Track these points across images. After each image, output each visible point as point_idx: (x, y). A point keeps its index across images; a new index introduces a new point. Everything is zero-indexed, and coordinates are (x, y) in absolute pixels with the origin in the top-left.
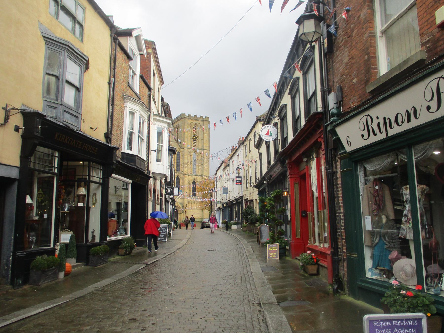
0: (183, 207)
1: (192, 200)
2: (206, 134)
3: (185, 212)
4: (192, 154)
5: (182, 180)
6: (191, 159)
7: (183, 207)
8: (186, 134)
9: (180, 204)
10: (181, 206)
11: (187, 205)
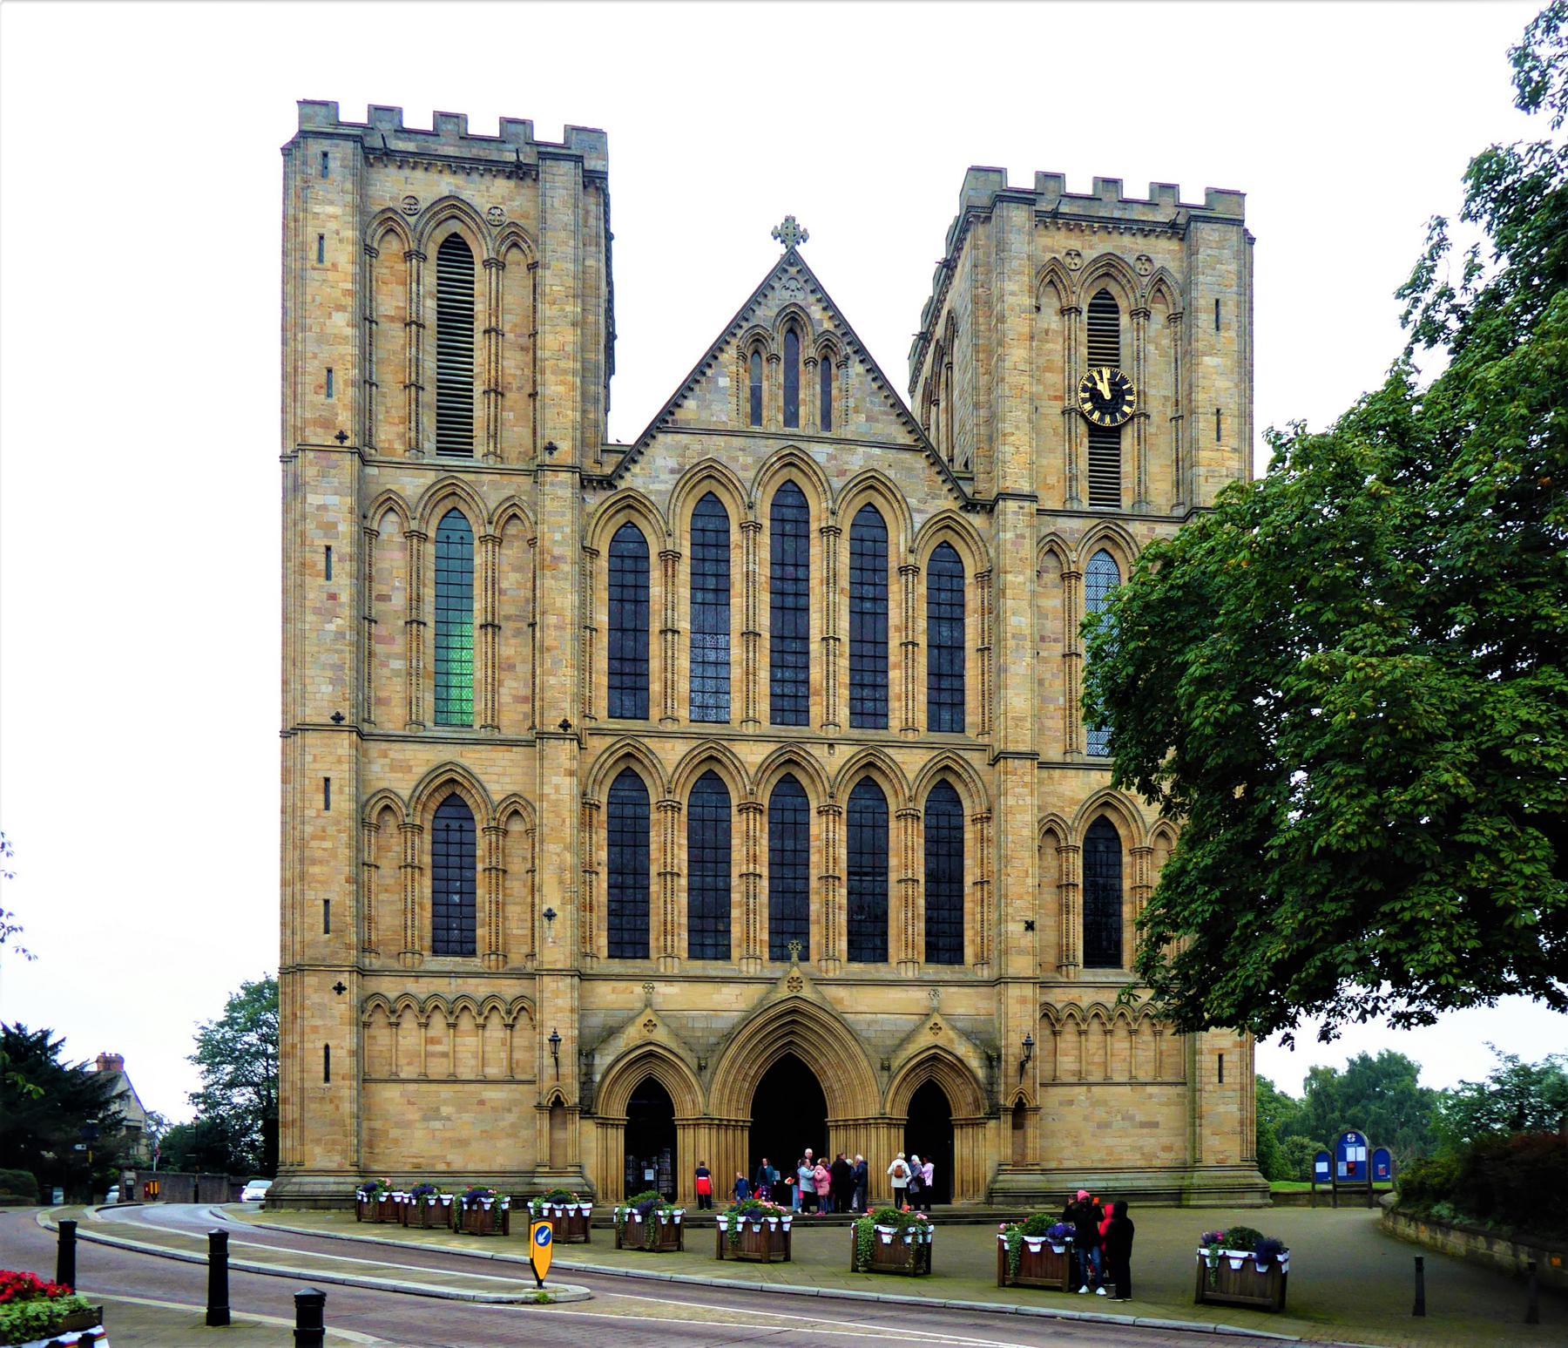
0: (992, 1060)
1: (1086, 998)
4: (1079, 558)
5: (980, 810)
6: (1069, 608)
7: (992, 1060)
9: (967, 1035)
10: (975, 1063)
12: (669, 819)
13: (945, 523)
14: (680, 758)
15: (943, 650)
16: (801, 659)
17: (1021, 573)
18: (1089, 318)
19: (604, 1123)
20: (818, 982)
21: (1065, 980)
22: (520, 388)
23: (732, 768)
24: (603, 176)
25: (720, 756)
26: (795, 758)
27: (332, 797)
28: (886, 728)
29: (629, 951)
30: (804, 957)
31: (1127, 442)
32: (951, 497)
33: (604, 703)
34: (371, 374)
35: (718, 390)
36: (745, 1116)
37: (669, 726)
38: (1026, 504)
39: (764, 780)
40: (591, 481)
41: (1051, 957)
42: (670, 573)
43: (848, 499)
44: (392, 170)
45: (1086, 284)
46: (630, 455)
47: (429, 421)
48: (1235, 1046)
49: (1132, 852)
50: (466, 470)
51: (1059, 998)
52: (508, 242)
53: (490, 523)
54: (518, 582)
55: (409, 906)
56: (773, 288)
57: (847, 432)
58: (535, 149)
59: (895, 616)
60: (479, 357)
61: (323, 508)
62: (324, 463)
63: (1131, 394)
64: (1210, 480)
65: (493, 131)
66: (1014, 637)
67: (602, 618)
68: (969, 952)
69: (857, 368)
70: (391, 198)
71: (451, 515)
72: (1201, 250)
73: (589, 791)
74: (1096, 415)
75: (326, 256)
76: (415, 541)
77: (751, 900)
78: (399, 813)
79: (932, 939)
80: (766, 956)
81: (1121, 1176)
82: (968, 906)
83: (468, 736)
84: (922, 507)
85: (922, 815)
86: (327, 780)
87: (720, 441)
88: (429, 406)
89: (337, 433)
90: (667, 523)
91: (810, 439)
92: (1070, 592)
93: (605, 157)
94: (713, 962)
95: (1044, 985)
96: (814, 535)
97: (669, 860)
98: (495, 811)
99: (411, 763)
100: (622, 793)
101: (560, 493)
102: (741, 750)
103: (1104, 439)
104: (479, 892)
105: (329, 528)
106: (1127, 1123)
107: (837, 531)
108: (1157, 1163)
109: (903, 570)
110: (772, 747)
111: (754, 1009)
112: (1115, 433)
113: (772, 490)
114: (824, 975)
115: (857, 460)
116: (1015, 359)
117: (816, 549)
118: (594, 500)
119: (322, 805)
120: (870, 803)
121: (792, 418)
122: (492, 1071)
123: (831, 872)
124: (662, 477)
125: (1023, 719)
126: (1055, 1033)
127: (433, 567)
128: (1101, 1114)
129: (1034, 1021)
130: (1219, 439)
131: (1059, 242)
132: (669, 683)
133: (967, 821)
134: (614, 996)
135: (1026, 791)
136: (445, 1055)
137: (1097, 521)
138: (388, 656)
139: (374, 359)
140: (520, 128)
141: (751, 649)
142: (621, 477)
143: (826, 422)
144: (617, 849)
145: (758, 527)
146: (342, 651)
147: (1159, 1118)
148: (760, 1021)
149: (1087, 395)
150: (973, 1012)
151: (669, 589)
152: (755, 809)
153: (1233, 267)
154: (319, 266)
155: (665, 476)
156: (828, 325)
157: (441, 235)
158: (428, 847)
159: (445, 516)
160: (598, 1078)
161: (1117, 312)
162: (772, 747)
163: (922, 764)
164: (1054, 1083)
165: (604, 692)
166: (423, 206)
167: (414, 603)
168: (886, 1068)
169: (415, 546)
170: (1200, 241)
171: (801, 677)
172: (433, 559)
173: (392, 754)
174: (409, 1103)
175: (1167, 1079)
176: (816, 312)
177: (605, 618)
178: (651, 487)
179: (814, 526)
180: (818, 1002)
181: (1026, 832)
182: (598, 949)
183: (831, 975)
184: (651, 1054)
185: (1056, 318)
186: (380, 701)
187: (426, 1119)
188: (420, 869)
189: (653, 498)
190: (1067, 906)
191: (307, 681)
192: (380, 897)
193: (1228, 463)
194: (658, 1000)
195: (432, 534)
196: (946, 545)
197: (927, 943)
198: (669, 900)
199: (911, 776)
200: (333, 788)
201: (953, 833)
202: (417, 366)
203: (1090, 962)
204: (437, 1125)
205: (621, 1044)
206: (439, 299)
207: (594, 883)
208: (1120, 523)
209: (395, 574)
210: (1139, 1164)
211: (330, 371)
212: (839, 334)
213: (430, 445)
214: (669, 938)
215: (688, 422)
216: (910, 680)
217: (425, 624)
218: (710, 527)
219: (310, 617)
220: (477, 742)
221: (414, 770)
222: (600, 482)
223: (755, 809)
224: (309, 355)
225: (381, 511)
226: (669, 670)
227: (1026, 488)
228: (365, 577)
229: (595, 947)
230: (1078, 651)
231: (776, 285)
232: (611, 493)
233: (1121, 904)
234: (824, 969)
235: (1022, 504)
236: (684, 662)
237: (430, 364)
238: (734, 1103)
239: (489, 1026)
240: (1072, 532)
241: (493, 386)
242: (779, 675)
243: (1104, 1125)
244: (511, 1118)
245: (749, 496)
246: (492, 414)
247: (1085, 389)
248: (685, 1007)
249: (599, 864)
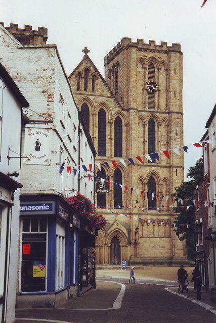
0: (129, 231)
3: (135, 242)
7: (129, 231)
11: (137, 228)
13: (118, 113)
28: (105, 156)
31: (156, 96)
49: (158, 185)
51: (143, 217)
57: (97, 93)
59: (108, 132)
65: (24, 28)
69: (100, 80)
82: (123, 196)
93: (47, 34)
95: (140, 214)
103: (151, 94)
106: (158, 247)
112: (153, 94)
113: (81, 105)
115: (100, 99)
117: (91, 118)
121: (85, 90)
126: (142, 225)
128: (152, 245)
131: (142, 54)
133: (123, 177)
143: (93, 91)
156: (94, 71)
164: (142, 237)
168: (106, 233)
175: (167, 236)
176: (91, 68)
179: (90, 113)
181: (136, 181)
196: (118, 117)
210: (161, 256)
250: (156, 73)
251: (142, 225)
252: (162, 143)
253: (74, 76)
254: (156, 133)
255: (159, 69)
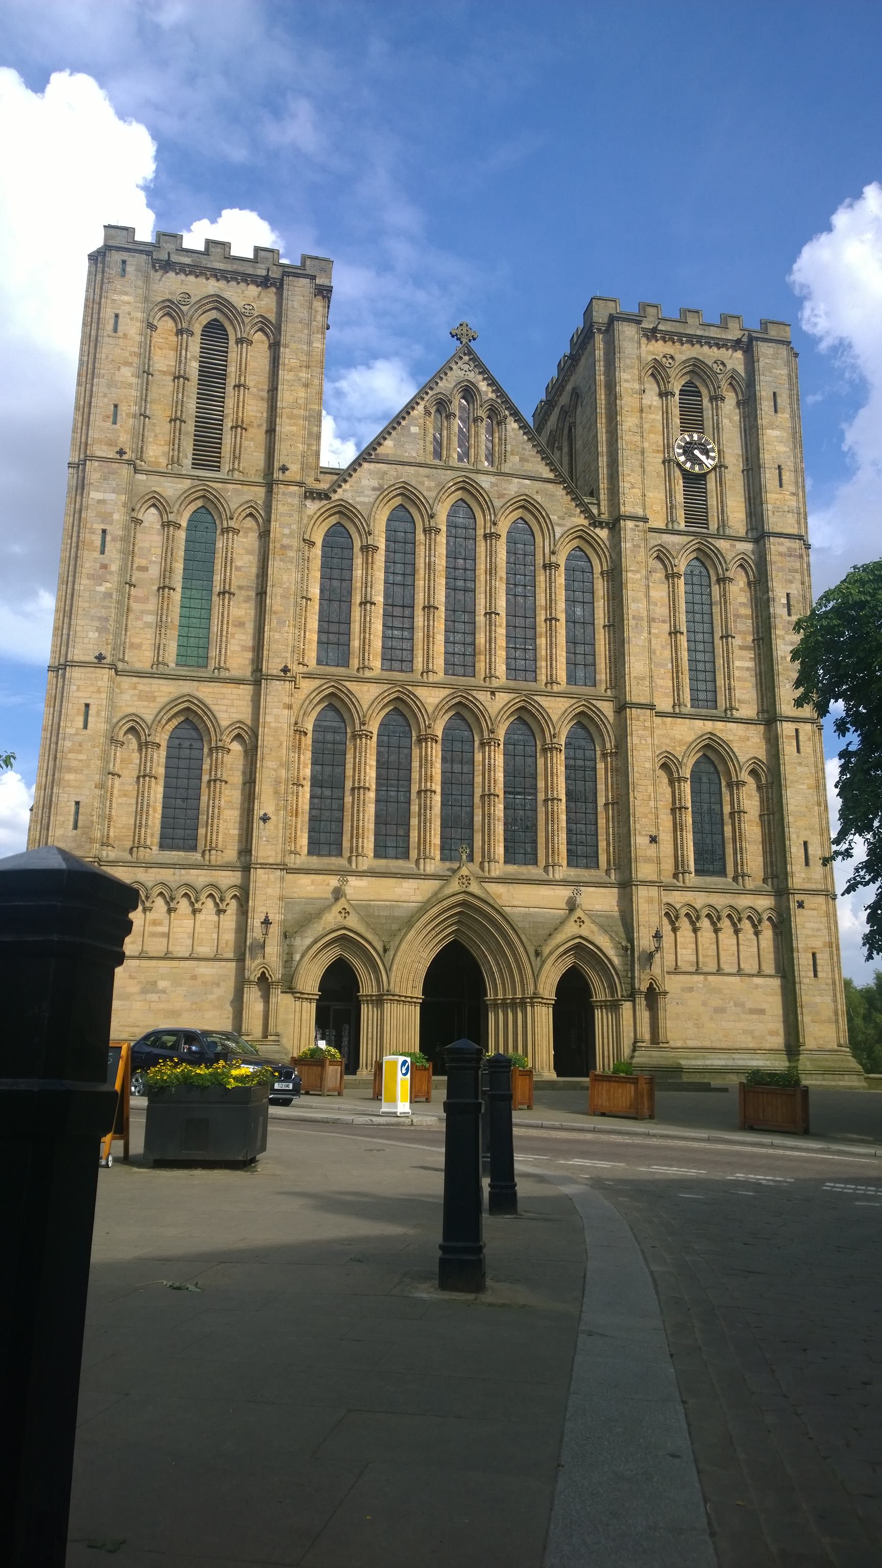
1: (700, 900)
2: (772, 426)
3: (651, 989)
8: (626, 426)
9: (604, 929)
11: (658, 936)
12: (364, 745)
14: (373, 698)
15: (577, 625)
16: (468, 628)
17: (638, 572)
18: (680, 399)
19: (299, 996)
20: (482, 880)
21: (682, 884)
22: (259, 426)
23: (414, 707)
24: (329, 290)
25: (405, 697)
26: (464, 701)
27: (90, 719)
28: (536, 681)
29: (325, 849)
30: (471, 858)
32: (582, 516)
33: (314, 655)
34: (145, 409)
35: (410, 435)
36: (418, 993)
37: (368, 674)
38: (641, 524)
39: (439, 717)
40: (312, 493)
41: (668, 865)
42: (370, 561)
43: (506, 514)
44: (171, 274)
45: (678, 377)
46: (342, 476)
47: (188, 446)
48: (825, 946)
49: (730, 785)
50: (215, 480)
51: (677, 899)
52: (256, 328)
53: (232, 519)
54: (250, 562)
55: (145, 809)
56: (451, 369)
57: (506, 468)
58: (281, 269)
59: (541, 600)
60: (230, 402)
61: (99, 501)
62: (106, 470)
63: (714, 452)
64: (776, 514)
66: (634, 617)
67: (315, 591)
68: (603, 858)
69: (512, 425)
70: (170, 293)
71: (200, 511)
72: (761, 359)
73: (300, 720)
74: (688, 465)
75: (120, 328)
76: (171, 528)
77: (428, 811)
78: (142, 733)
79: (570, 847)
80: (438, 857)
81: (736, 1056)
83: (203, 675)
84: (561, 522)
85: (563, 748)
86: (87, 706)
87: (412, 470)
88: (187, 433)
89: (118, 449)
90: (368, 525)
91: (478, 472)
92: (673, 588)
94: (394, 861)
95: (668, 888)
96: (480, 538)
97: (362, 778)
98: (221, 734)
99: (156, 694)
100: (325, 724)
101: (289, 500)
102: (421, 692)
104: (204, 798)
105: (106, 517)
107: (498, 536)
108: (767, 1046)
109: (548, 566)
110: (448, 691)
111: (429, 900)
112: (703, 477)
114: (487, 874)
115: (513, 487)
116: (629, 424)
118: (312, 507)
119: (81, 725)
120: (521, 737)
122: (205, 950)
123: (492, 790)
124: (366, 492)
125: (643, 679)
126: (675, 930)
127: (183, 548)
128: (716, 1002)
129: (660, 917)
130: (781, 486)
132: (367, 641)
134: (313, 887)
135: (648, 733)
136: (163, 935)
137: (692, 538)
138: (143, 612)
139: (149, 399)
140: (270, 255)
141: (431, 618)
142: (335, 492)
144: (319, 768)
145: (438, 531)
146: (110, 607)
147: (764, 1006)
148: (435, 910)
149: (681, 451)
150: (607, 908)
151: (370, 571)
152: (432, 739)
153: (785, 372)
154: (114, 335)
155: (367, 492)
156: (492, 395)
157: (205, 319)
158: (163, 760)
159: (195, 512)
160: (297, 957)
161: (700, 396)
162: (448, 691)
163: (564, 709)
164: (676, 971)
165: (314, 646)
166: (193, 300)
167: (167, 574)
168: (537, 954)
169: (171, 533)
170: (760, 354)
171: (469, 639)
172: (183, 543)
173: (140, 687)
174: (131, 977)
176: (483, 386)
177: (318, 591)
178: (357, 499)
179: (480, 532)
180: (483, 896)
181: (648, 765)
182: (301, 848)
183: (493, 874)
184: (343, 938)
185: (657, 398)
186: (132, 646)
187: (144, 991)
188: (156, 778)
189: (358, 507)
190: (681, 825)
191: (78, 628)
192: (120, 800)
193: (788, 503)
194: (349, 891)
195: (184, 524)
197: (568, 850)
198: (361, 809)
199: (555, 718)
200: (92, 711)
201: (588, 763)
202: (182, 406)
203: (699, 872)
204: (154, 997)
205: (318, 928)
206: (200, 362)
207: (300, 794)
208: (709, 540)
209: (153, 551)
210: (751, 1045)
211: (116, 406)
212: (499, 401)
213: (188, 461)
214: (360, 840)
215: (387, 455)
216: (554, 645)
217: (174, 590)
218: (401, 529)
219: (85, 581)
220: (212, 680)
221: (158, 700)
222: (319, 494)
223: (432, 739)
224: (100, 394)
225: (146, 506)
226: (367, 631)
227: (640, 513)
228: (129, 553)
229: (298, 846)
230: (681, 630)
231: (454, 367)
232: (325, 502)
233: (723, 825)
234: (486, 869)
235: (636, 523)
236: (378, 626)
237: (191, 405)
238: (410, 982)
239: (204, 911)
240: (674, 545)
241: (240, 423)
242: (452, 639)
243: (719, 1010)
244: (219, 992)
245: (432, 509)
246: (238, 442)
247: (680, 447)
248: (372, 898)
249: (304, 779)
250: (708, 413)
251: (675, 930)
252: (737, 642)
253: (420, 408)
254: (716, 609)
255: (716, 398)
